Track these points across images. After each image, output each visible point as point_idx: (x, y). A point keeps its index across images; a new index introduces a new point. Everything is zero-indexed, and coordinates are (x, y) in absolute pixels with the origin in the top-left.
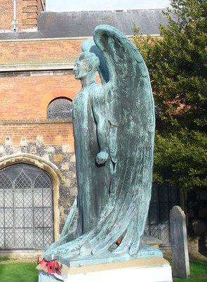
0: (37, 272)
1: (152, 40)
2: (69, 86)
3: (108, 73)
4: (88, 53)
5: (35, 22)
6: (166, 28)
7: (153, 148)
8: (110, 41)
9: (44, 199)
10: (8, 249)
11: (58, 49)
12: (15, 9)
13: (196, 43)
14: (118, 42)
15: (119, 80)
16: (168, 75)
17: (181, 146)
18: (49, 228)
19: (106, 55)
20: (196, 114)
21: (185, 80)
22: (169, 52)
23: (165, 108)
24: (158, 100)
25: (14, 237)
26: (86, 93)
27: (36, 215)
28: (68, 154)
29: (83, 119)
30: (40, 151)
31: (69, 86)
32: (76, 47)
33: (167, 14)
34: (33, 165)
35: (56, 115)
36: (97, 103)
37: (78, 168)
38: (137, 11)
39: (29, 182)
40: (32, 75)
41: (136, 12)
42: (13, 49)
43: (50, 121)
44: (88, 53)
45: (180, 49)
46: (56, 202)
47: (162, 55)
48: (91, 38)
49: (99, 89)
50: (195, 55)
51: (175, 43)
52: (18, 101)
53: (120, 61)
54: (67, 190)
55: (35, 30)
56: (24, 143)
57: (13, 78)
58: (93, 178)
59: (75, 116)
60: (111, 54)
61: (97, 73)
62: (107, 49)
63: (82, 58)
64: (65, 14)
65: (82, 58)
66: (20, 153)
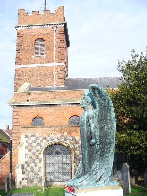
0: (65, 191)
1: (115, 91)
2: (78, 111)
3: (95, 105)
4: (86, 96)
5: (64, 83)
6: (121, 86)
7: (115, 138)
8: (96, 91)
9: (68, 160)
10: (52, 182)
11: (73, 95)
12: (54, 77)
13: (134, 92)
14: (99, 92)
15: (100, 108)
16: (121, 106)
17: (127, 137)
18: (70, 172)
19: (94, 97)
20: (134, 123)
21: (129, 108)
22: (122, 96)
23: (120, 120)
24: (117, 117)
25: (54, 176)
26: (86, 113)
27: (64, 167)
28: (78, 140)
29: (84, 125)
30: (66, 139)
31: (78, 111)
32: (81, 94)
33: (121, 79)
34: (62, 145)
35: (72, 123)
36: (90, 118)
37: (82, 146)
38: (108, 78)
39: (61, 152)
40: (62, 106)
41: (107, 78)
42: (54, 94)
43: (70, 126)
44: (86, 96)
45: (126, 95)
46: (73, 161)
47: (119, 97)
48: (88, 90)
49: (91, 112)
50: (133, 97)
51: (125, 92)
52: (56, 117)
53: (100, 100)
54: (77, 156)
55: (63, 86)
56: (59, 135)
57: (54, 107)
58: (89, 151)
59: (81, 124)
60: (97, 96)
61: (90, 105)
62: (95, 95)
63: (84, 98)
64: (77, 79)
65: (84, 98)
66: (57, 140)
